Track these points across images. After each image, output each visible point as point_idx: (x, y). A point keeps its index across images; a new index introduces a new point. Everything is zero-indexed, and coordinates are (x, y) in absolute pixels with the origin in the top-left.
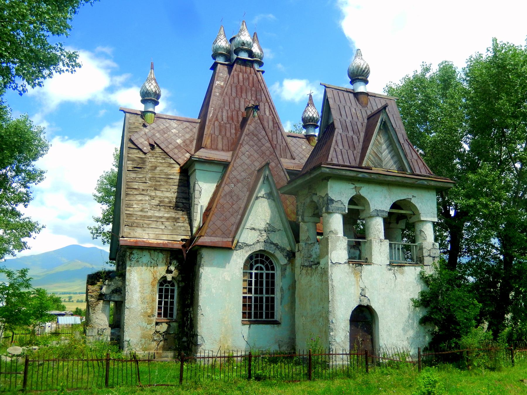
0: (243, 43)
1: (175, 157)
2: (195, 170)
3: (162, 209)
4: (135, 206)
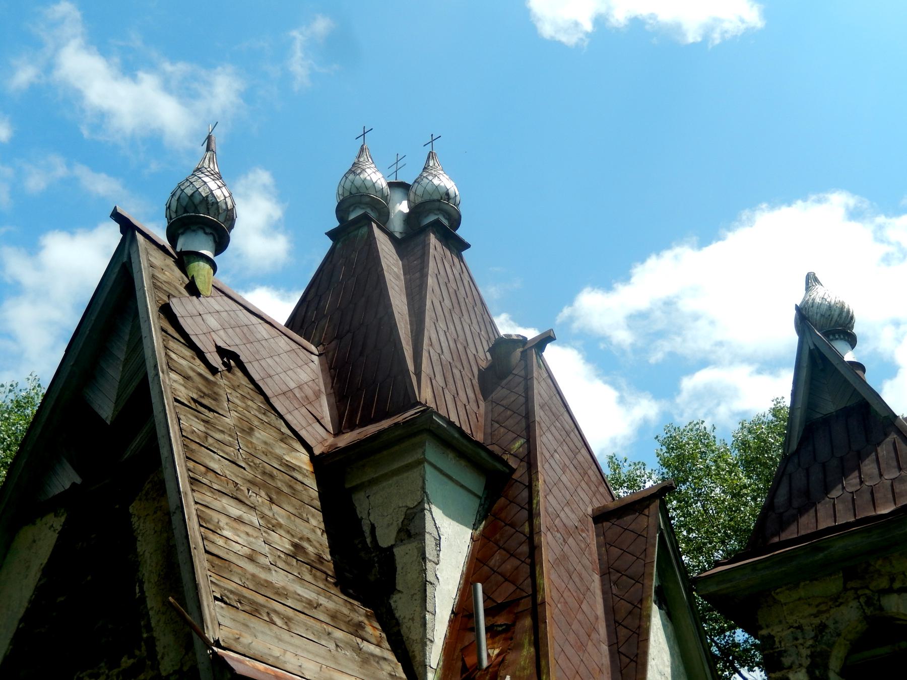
0: (447, 194)
1: (288, 417)
2: (420, 462)
3: (308, 577)
4: (226, 533)
